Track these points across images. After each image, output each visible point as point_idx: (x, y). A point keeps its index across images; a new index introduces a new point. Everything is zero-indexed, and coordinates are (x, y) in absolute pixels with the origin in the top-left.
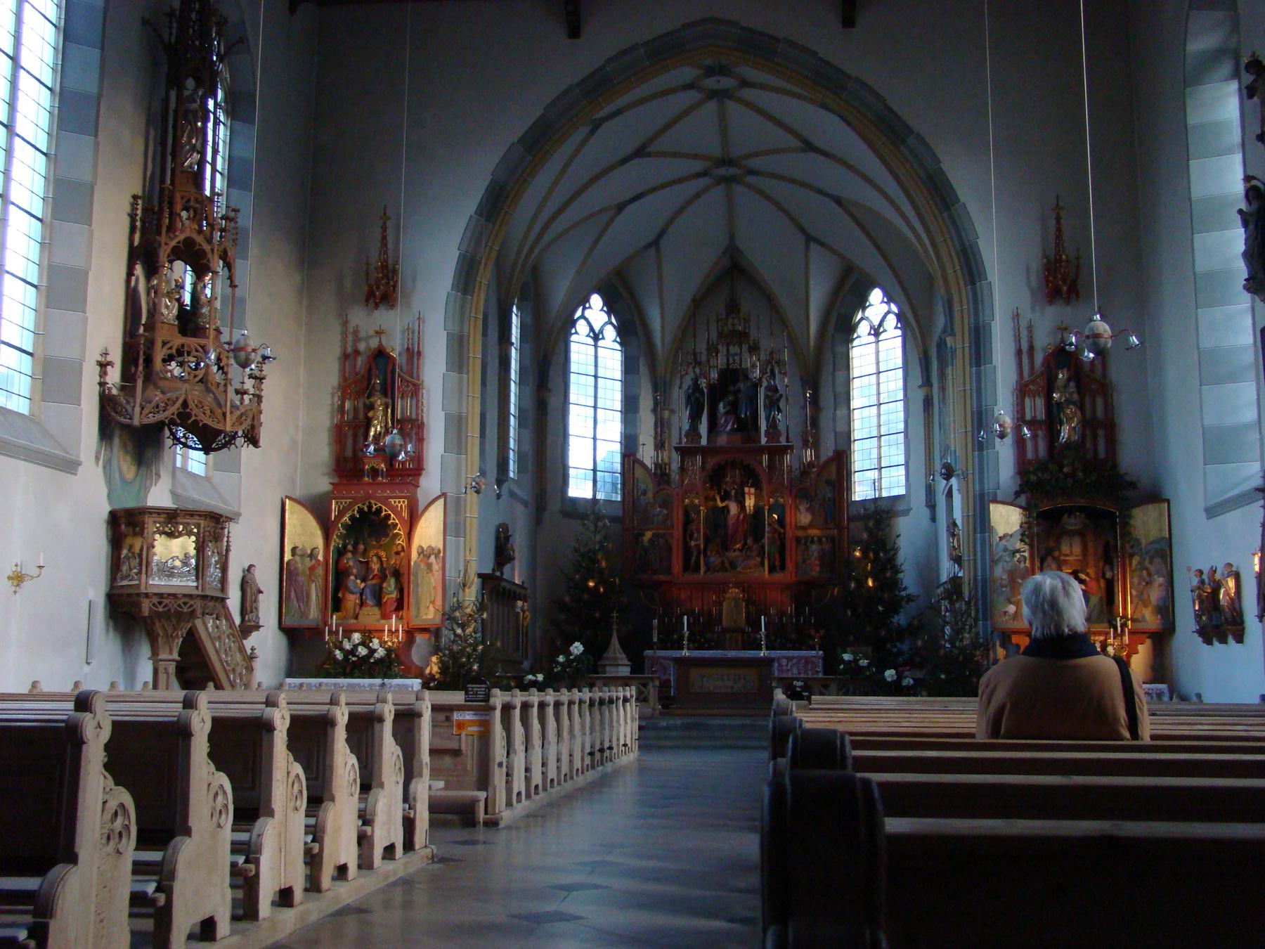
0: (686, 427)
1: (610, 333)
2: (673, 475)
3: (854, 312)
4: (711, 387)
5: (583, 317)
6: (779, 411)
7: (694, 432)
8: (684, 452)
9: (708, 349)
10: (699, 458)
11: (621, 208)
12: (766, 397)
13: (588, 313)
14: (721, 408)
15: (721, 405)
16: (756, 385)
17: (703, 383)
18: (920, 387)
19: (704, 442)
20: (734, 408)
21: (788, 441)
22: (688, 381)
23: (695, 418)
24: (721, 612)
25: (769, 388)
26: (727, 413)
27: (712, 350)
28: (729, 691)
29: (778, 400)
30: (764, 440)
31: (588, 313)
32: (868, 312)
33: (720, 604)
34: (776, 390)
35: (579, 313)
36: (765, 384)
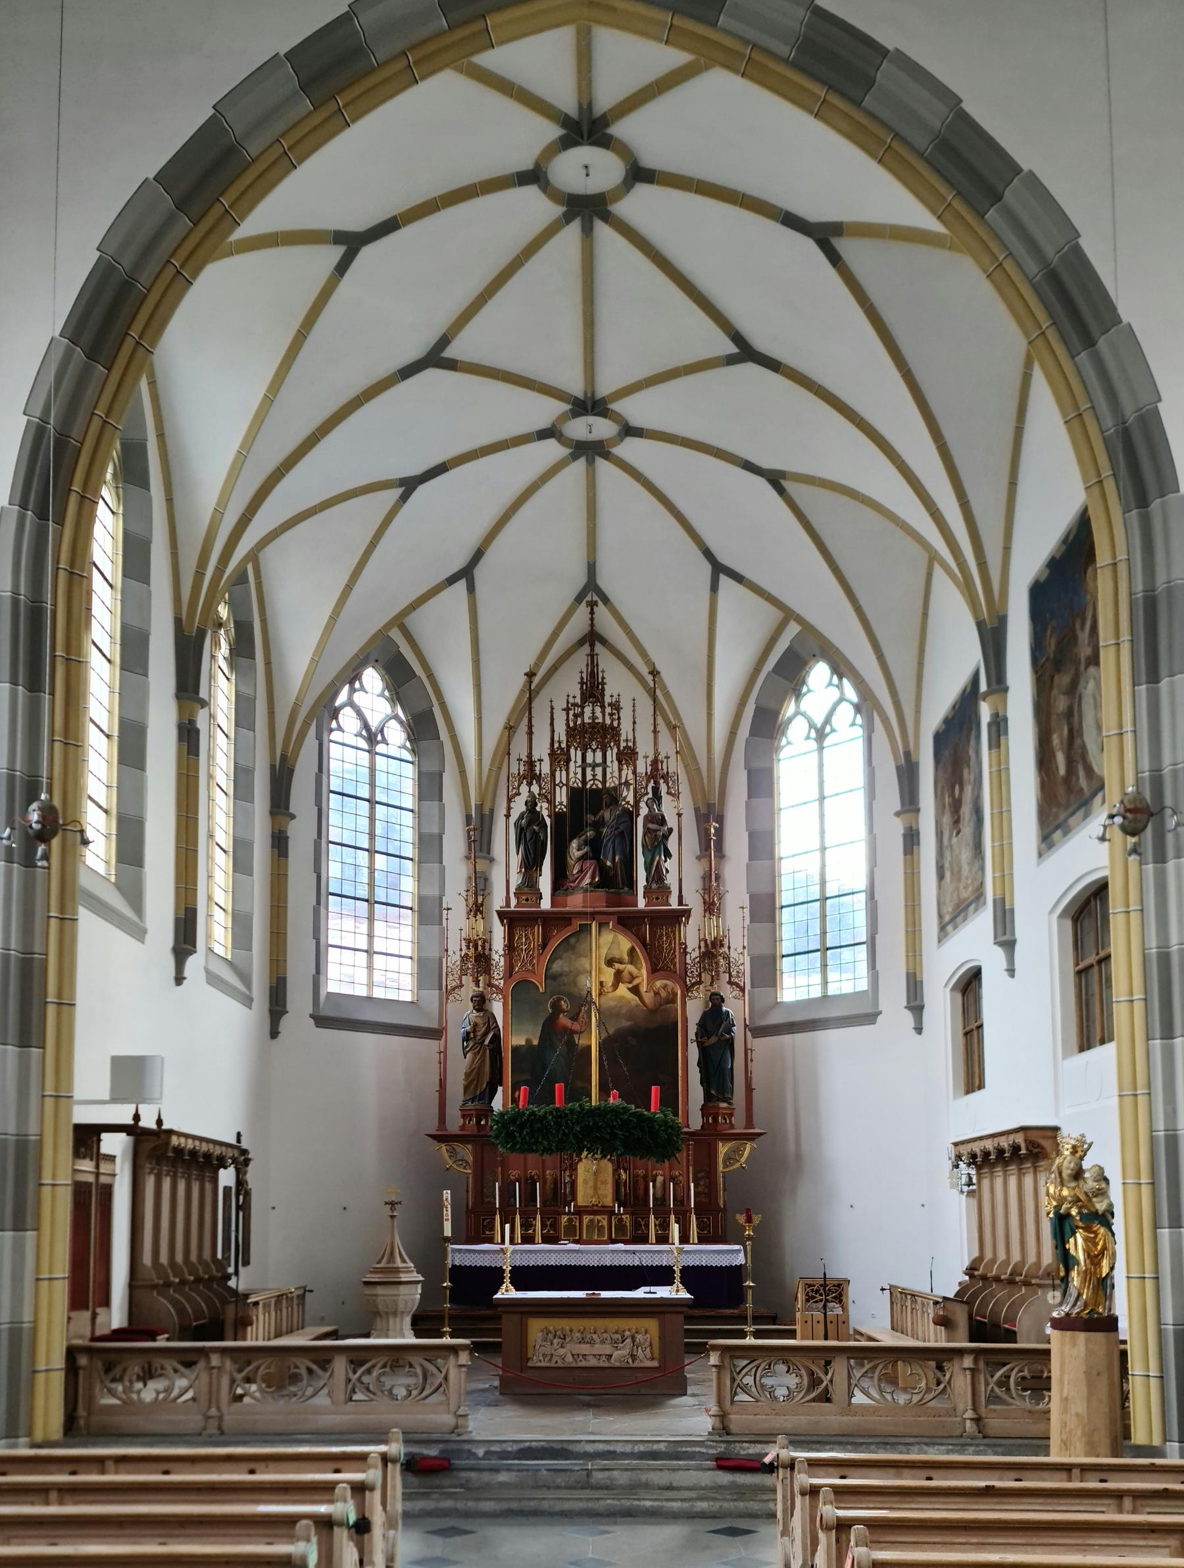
0: (516, 879)
1: (396, 735)
2: (495, 957)
3: (781, 701)
4: (557, 817)
5: (350, 703)
6: (668, 855)
7: (529, 886)
8: (510, 919)
9: (552, 754)
10: (538, 930)
11: (409, 485)
12: (647, 830)
13: (358, 698)
14: (575, 850)
15: (574, 844)
16: (630, 816)
17: (543, 808)
18: (897, 814)
19: (546, 904)
20: (595, 849)
21: (680, 903)
22: (519, 807)
23: (531, 865)
24: (573, 1184)
25: (650, 819)
26: (583, 858)
27: (559, 757)
28: (603, 1363)
29: (666, 837)
30: (641, 903)
31: (358, 698)
32: (806, 703)
33: (573, 1168)
34: (662, 821)
35: (342, 697)
36: (644, 811)
